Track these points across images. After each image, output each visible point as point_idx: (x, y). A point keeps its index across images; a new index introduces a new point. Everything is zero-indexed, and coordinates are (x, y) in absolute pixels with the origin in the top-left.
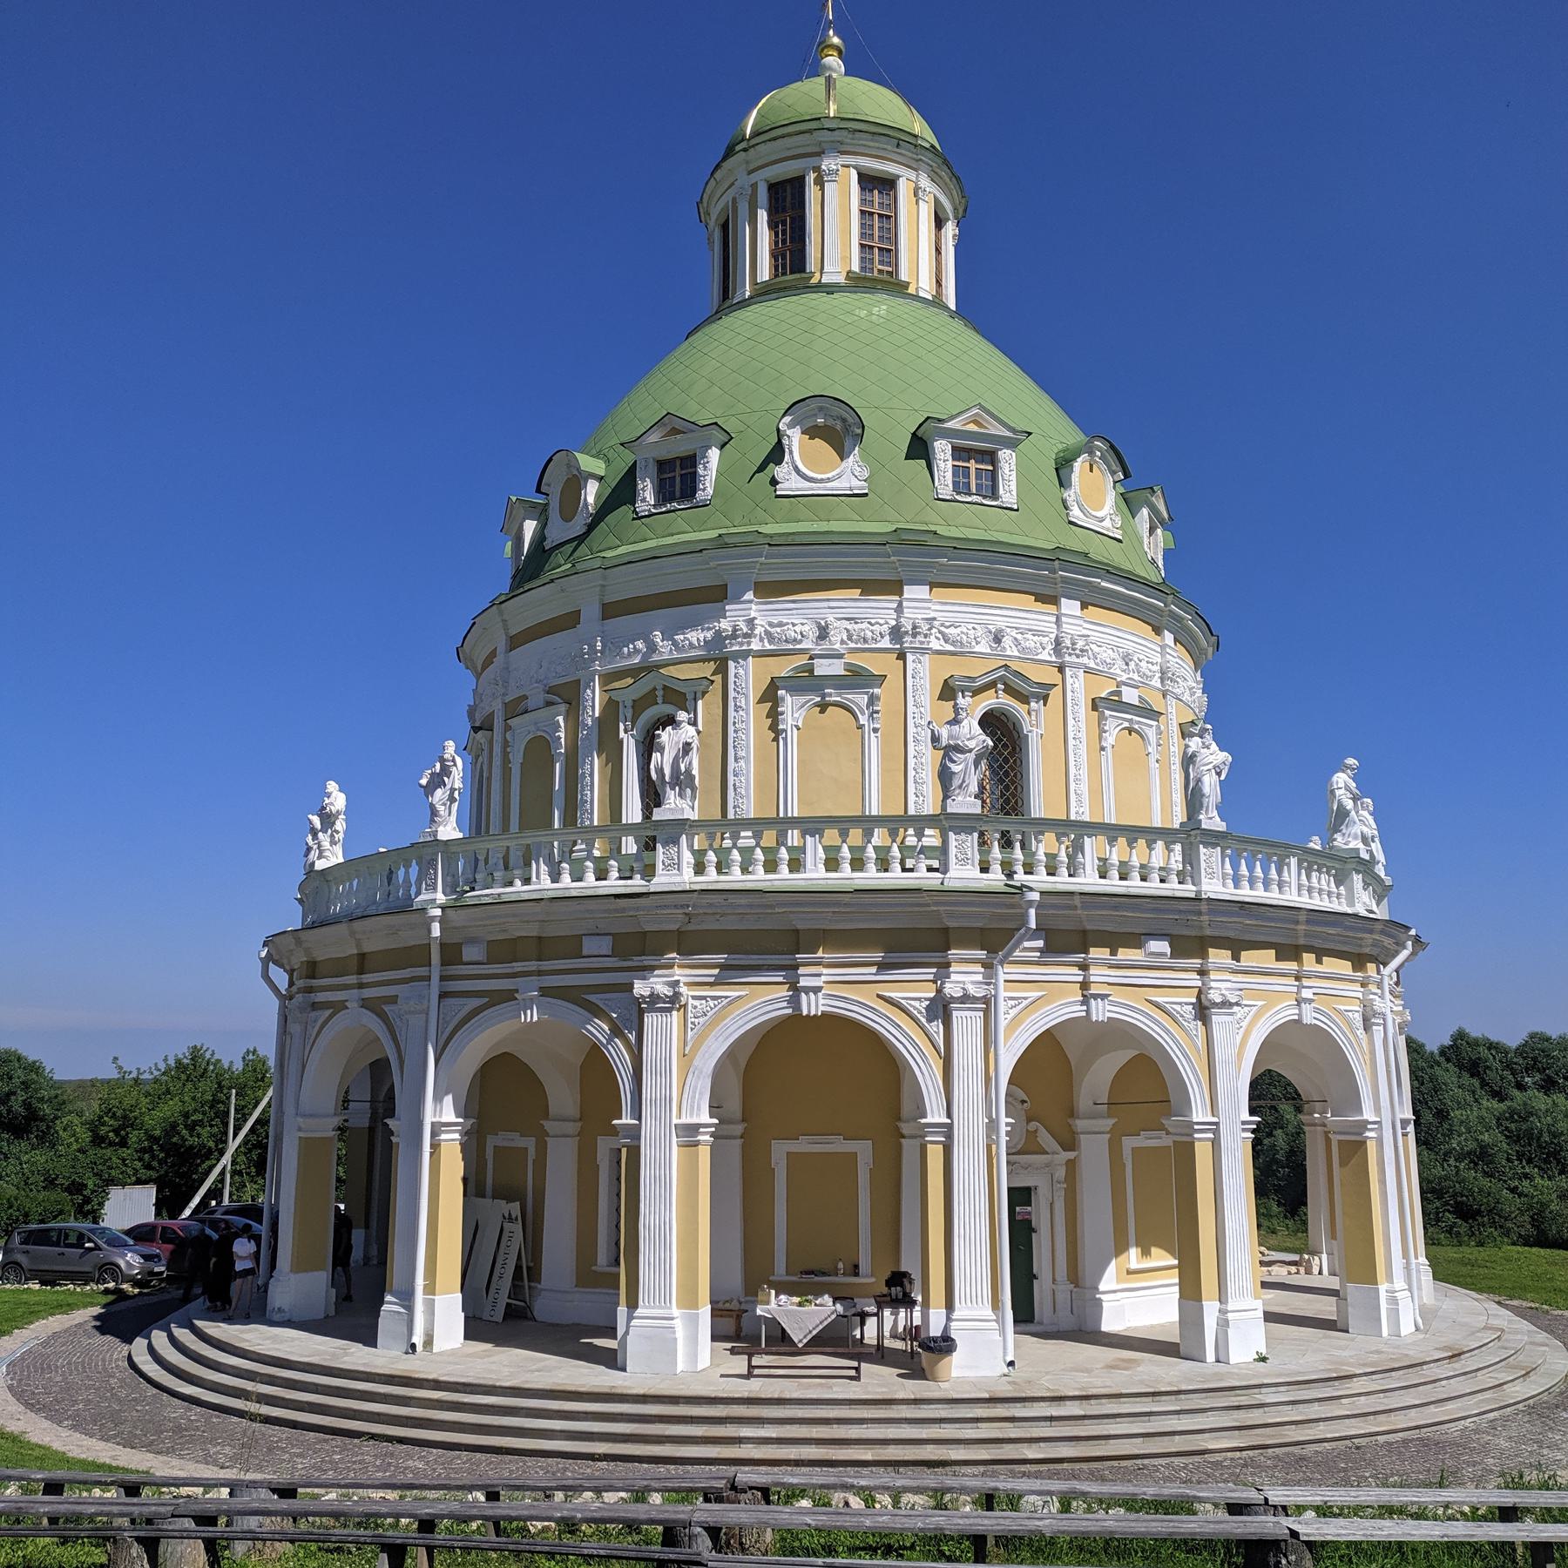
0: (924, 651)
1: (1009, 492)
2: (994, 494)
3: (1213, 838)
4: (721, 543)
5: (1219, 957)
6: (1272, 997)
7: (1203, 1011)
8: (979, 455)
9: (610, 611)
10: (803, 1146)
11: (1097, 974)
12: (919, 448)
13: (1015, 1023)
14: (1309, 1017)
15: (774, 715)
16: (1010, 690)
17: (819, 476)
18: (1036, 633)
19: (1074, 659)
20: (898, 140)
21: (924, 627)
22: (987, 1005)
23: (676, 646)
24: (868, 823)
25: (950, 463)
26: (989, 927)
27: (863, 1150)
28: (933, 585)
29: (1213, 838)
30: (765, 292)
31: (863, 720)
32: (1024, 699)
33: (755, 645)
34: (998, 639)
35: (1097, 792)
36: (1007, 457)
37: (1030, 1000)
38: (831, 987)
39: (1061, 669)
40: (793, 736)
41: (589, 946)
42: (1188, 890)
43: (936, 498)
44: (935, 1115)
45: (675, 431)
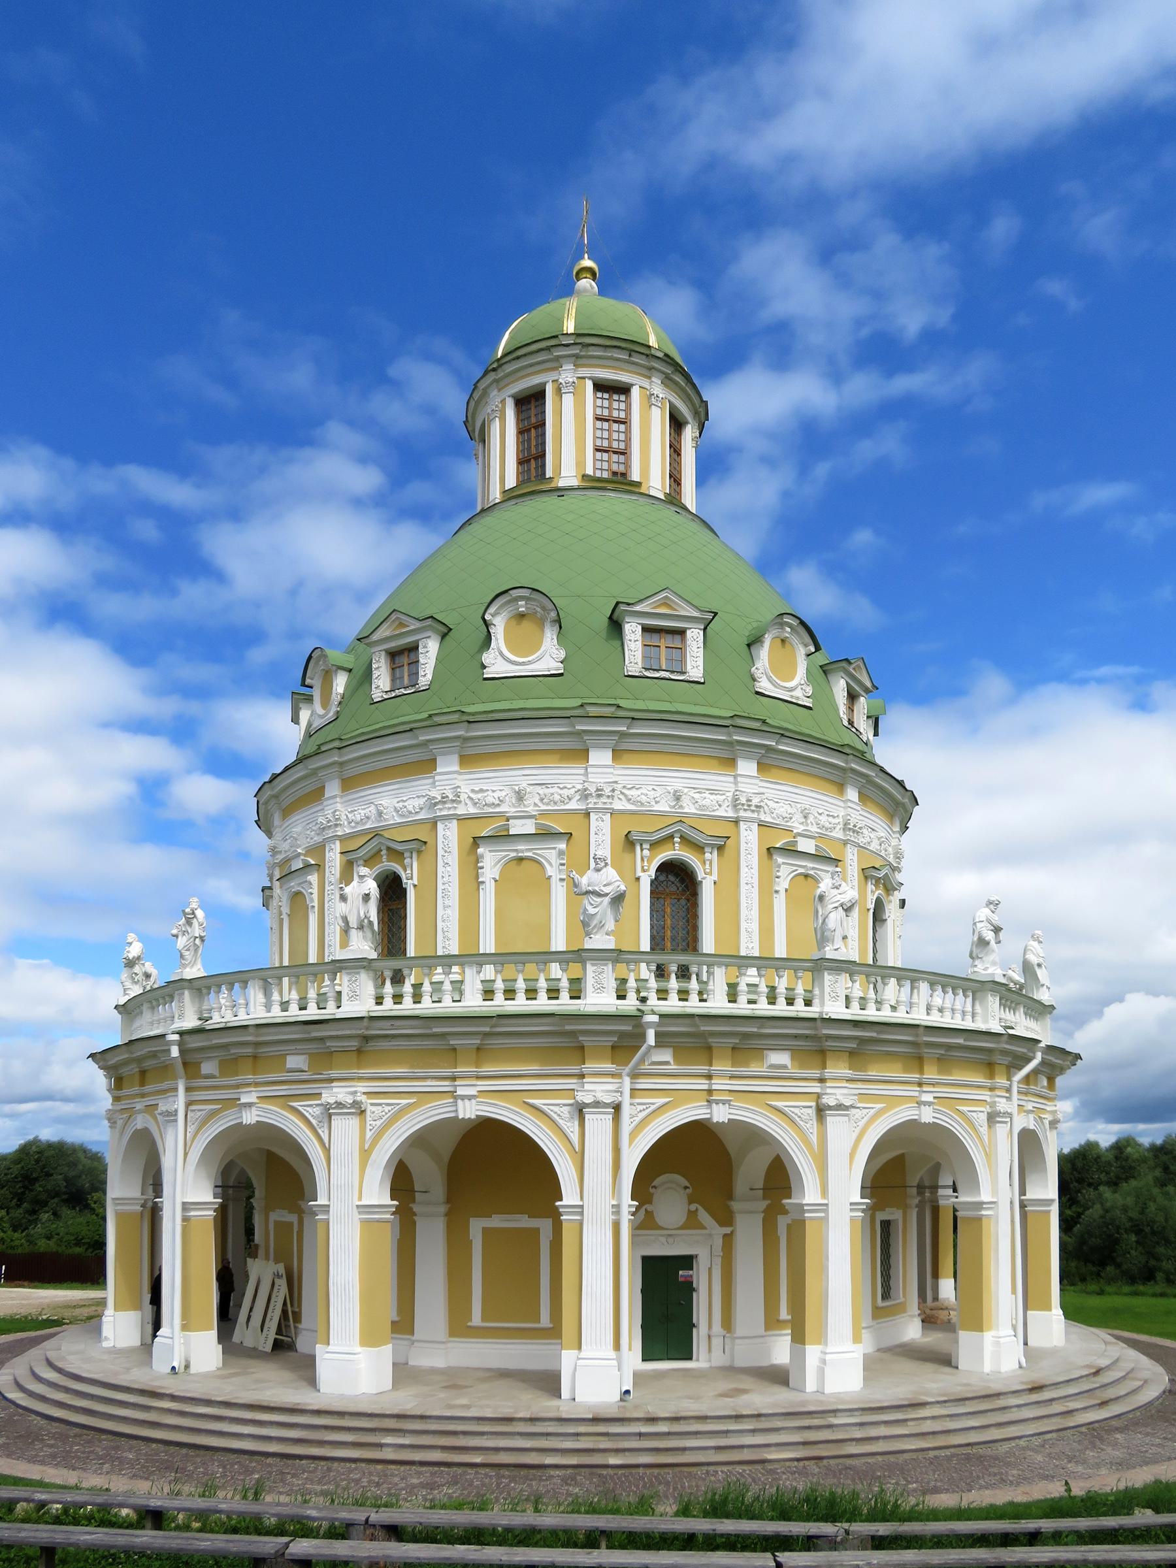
0: (604, 810)
5: (838, 1069)
7: (821, 1111)
14: (927, 1116)
16: (686, 841)
17: (530, 659)
18: (713, 792)
19: (749, 814)
21: (607, 791)
22: (617, 1108)
24: (545, 957)
25: (639, 644)
31: (550, 871)
32: (699, 848)
34: (678, 799)
35: (767, 931)
39: (736, 822)
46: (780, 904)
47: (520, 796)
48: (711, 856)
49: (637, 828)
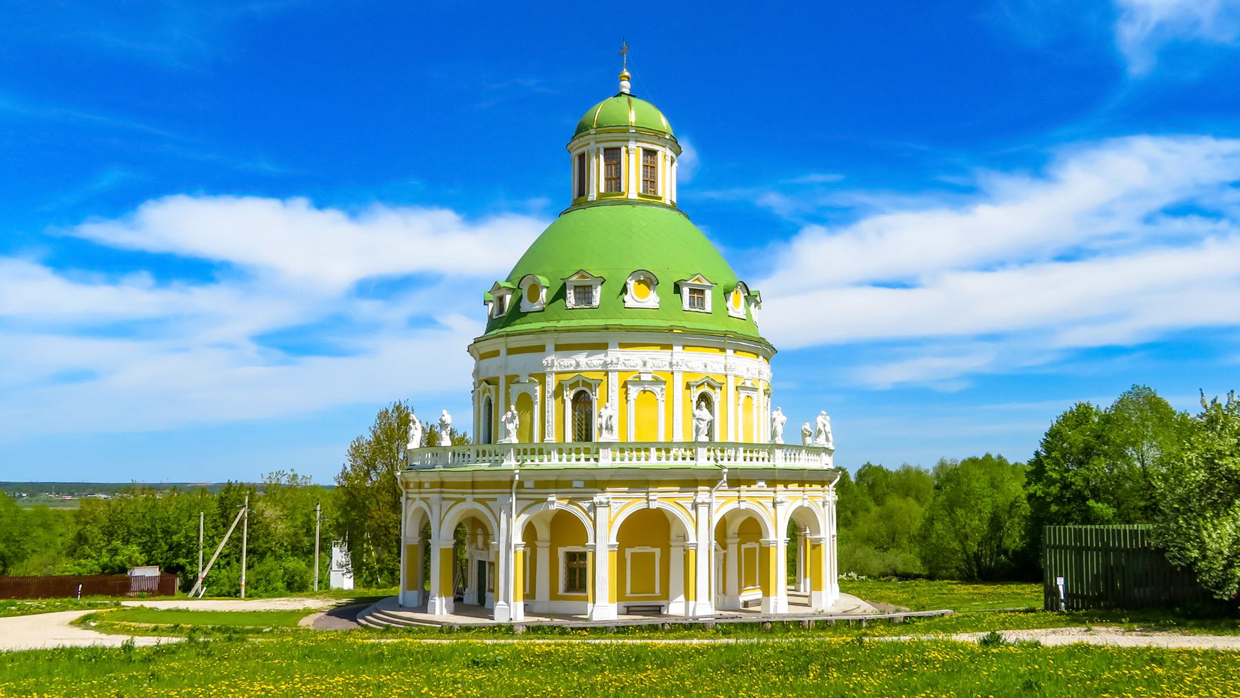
1: (708, 308)
2: (702, 305)
3: (780, 447)
4: (606, 328)
5: (780, 487)
6: (796, 498)
7: (774, 504)
8: (698, 292)
9: (559, 348)
10: (637, 550)
11: (742, 494)
12: (677, 289)
13: (718, 509)
15: (626, 393)
16: (709, 385)
20: (658, 135)
23: (585, 361)
26: (711, 480)
27: (657, 551)
28: (684, 347)
29: (780, 447)
30: (601, 201)
31: (659, 397)
32: (713, 388)
33: (619, 367)
36: (708, 293)
37: (722, 502)
38: (660, 499)
40: (632, 403)
41: (575, 484)
42: (770, 465)
43: (684, 314)
44: (692, 540)
45: (583, 277)
46: (740, 408)
47: (645, 364)
48: (718, 390)
49: (692, 380)
